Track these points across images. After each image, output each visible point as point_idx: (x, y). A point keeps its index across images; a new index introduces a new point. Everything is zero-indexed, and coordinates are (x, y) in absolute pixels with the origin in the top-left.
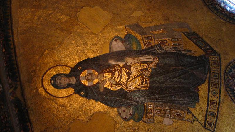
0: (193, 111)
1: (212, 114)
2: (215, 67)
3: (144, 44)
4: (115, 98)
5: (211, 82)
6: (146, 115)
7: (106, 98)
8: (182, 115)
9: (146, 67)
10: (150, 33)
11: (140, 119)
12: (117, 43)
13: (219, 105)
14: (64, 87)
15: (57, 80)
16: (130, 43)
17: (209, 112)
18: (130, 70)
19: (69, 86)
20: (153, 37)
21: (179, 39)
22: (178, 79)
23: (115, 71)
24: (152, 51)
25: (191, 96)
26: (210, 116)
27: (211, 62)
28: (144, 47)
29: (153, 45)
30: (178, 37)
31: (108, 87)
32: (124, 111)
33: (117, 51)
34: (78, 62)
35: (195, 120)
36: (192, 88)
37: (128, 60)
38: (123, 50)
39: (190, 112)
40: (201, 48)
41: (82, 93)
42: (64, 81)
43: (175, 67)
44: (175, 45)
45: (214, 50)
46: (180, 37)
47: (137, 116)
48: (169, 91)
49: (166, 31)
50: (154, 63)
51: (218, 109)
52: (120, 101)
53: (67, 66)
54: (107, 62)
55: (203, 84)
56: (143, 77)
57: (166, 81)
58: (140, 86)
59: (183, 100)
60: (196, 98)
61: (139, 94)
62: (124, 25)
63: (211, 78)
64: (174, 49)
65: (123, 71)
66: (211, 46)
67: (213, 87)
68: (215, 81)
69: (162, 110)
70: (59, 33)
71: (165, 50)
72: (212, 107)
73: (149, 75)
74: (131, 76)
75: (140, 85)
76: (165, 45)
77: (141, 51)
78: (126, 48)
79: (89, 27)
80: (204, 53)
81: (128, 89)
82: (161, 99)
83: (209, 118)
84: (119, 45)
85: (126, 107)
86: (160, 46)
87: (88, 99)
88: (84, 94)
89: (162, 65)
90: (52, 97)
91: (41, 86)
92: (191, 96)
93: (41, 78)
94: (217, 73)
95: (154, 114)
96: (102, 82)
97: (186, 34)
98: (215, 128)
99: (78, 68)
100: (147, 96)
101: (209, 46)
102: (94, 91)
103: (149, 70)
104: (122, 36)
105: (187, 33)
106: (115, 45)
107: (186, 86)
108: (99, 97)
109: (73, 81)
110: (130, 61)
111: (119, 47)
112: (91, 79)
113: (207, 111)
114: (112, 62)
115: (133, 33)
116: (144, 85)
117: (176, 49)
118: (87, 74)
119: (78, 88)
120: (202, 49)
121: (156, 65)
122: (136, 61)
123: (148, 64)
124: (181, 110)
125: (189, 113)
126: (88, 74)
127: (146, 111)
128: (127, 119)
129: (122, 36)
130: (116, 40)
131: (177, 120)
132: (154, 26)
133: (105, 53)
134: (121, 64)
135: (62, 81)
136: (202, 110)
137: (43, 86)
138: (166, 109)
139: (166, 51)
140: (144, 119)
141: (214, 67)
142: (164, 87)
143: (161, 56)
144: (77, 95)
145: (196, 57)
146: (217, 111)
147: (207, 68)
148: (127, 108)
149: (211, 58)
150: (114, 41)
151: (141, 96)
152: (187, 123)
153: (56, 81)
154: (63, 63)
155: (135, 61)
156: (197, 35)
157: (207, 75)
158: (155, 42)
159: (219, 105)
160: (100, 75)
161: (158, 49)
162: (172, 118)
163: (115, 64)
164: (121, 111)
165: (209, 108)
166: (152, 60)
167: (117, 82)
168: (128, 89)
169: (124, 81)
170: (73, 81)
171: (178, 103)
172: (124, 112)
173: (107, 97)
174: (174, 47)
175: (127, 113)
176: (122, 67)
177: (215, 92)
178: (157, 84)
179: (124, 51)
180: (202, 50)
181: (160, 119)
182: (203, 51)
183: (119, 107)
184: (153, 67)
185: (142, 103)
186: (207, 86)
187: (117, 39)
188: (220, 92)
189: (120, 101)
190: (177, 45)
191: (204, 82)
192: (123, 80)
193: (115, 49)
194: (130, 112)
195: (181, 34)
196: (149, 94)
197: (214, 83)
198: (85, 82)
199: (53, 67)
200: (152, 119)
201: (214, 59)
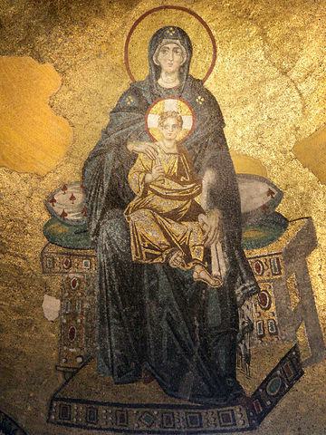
7: (110, 156)
11: (51, 238)
14: (154, 59)
18: (185, 219)
23: (183, 183)
24: (241, 274)
30: (282, 335)
32: (72, 198)
33: (241, 193)
45: (265, 416)
48: (133, 311)
50: (208, 278)
51: (107, 429)
52: (101, 190)
55: (165, 391)
56: (166, 249)
59: (114, 345)
69: (80, 294)
73: (171, 265)
76: (256, 306)
93: (188, 7)
96: (153, 150)
98: (59, 424)
100: (115, 257)
101: (273, 406)
102: (132, 127)
106: (257, 190)
107: (152, 353)
109: (168, 81)
110: (211, 221)
111: (252, 198)
112: (165, 123)
115: (292, 231)
122: (210, 236)
124: (86, 340)
125: (80, 360)
129: (282, 209)
130: (270, 193)
134: (202, 200)
140: (53, 249)
144: (125, 87)
145: (233, 375)
148: (81, 205)
156: (298, 379)
160: (173, 147)
161: (245, 288)
166: (215, 272)
168: (134, 211)
169: (154, 203)
170: (168, 81)
171: (102, 334)
173: (111, 159)
174: (253, 324)
178: (149, 282)
180: (258, 390)
183: (82, 186)
184: (195, 276)
192: (157, 202)
201: (239, 416)
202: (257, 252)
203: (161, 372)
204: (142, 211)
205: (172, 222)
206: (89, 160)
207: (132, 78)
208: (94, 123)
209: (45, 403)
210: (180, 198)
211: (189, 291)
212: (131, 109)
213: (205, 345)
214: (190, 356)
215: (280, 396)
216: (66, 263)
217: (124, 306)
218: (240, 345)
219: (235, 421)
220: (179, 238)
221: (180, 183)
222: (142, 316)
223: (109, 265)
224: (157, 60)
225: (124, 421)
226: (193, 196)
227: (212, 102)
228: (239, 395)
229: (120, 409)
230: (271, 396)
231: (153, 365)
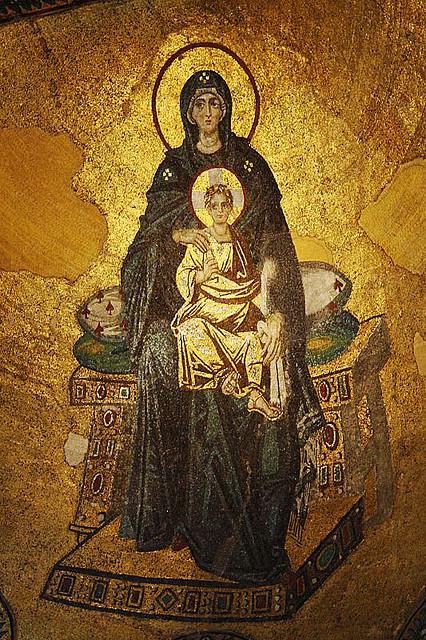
0: (111, 530)
1: (99, 592)
7: (153, 251)
9: (250, 380)
11: (83, 358)
13: (129, 614)
15: (211, 93)
16: (328, 331)
17: (107, 583)
18: (244, 327)
19: (192, 130)
22: (213, 484)
23: (239, 281)
24: (304, 401)
27: (267, 590)
28: (315, 375)
29: (323, 405)
31: (187, 255)
32: (110, 307)
34: (269, 159)
37: (274, 323)
39: (106, 522)
40: (313, 557)
41: (168, 174)
42: (207, 116)
48: (175, 454)
49: (366, 448)
52: (143, 295)
53: (255, 124)
54: (269, 255)
56: (220, 370)
57: (206, 445)
58: (190, 360)
63: (216, 590)
64: (308, 470)
65: (237, 308)
67: (187, 596)
68: (205, 601)
70: (361, 100)
73: (224, 391)
74: (223, 331)
75: (193, 360)
76: (321, 444)
77: (304, 367)
78: (313, 315)
79: (380, 198)
80: (295, 568)
85: (124, 315)
87: (147, 193)
90: (155, 75)
91: (191, 39)
93: (218, 40)
96: (203, 240)
97: (357, 510)
98: (55, 600)
100: (159, 383)
101: (319, 585)
104: (350, 306)
106: (323, 282)
109: (208, 145)
110: (272, 328)
112: (213, 202)
113: (110, 575)
114: (268, 270)
115: (362, 338)
116: (194, 373)
122: (270, 351)
124: (113, 492)
126: (230, 194)
127: (109, 381)
129: (350, 306)
130: (338, 285)
131: (79, 477)
134: (261, 301)
137: (193, 46)
138: (116, 442)
139: (302, 447)
140: (85, 374)
143: (286, 428)
144: (161, 157)
145: (282, 542)
150: (337, 277)
152: (71, 510)
153: (209, 89)
154: (265, 112)
157: (223, 576)
158: (327, 409)
159: (129, 614)
161: (308, 419)
166: (274, 399)
167: (203, 287)
168: (182, 321)
169: (205, 309)
170: (208, 145)
171: (134, 484)
176: (251, 304)
178: (197, 415)
180: (307, 562)
181: (84, 424)
185: (135, 366)
186: (189, 578)
187: (342, 289)
188: (169, 618)
189: (143, 295)
191: (203, 568)
193: (310, 280)
194: (106, 327)
197: (199, 598)
198: (203, 181)
199: (252, 80)
201: (277, 598)
202: (325, 369)
210: (238, 301)
211: (242, 426)
213: (256, 499)
215: (328, 573)
216: (100, 392)
219: (270, 605)
220: (235, 355)
221: (236, 280)
224: (191, 117)
226: (244, 300)
227: (262, 166)
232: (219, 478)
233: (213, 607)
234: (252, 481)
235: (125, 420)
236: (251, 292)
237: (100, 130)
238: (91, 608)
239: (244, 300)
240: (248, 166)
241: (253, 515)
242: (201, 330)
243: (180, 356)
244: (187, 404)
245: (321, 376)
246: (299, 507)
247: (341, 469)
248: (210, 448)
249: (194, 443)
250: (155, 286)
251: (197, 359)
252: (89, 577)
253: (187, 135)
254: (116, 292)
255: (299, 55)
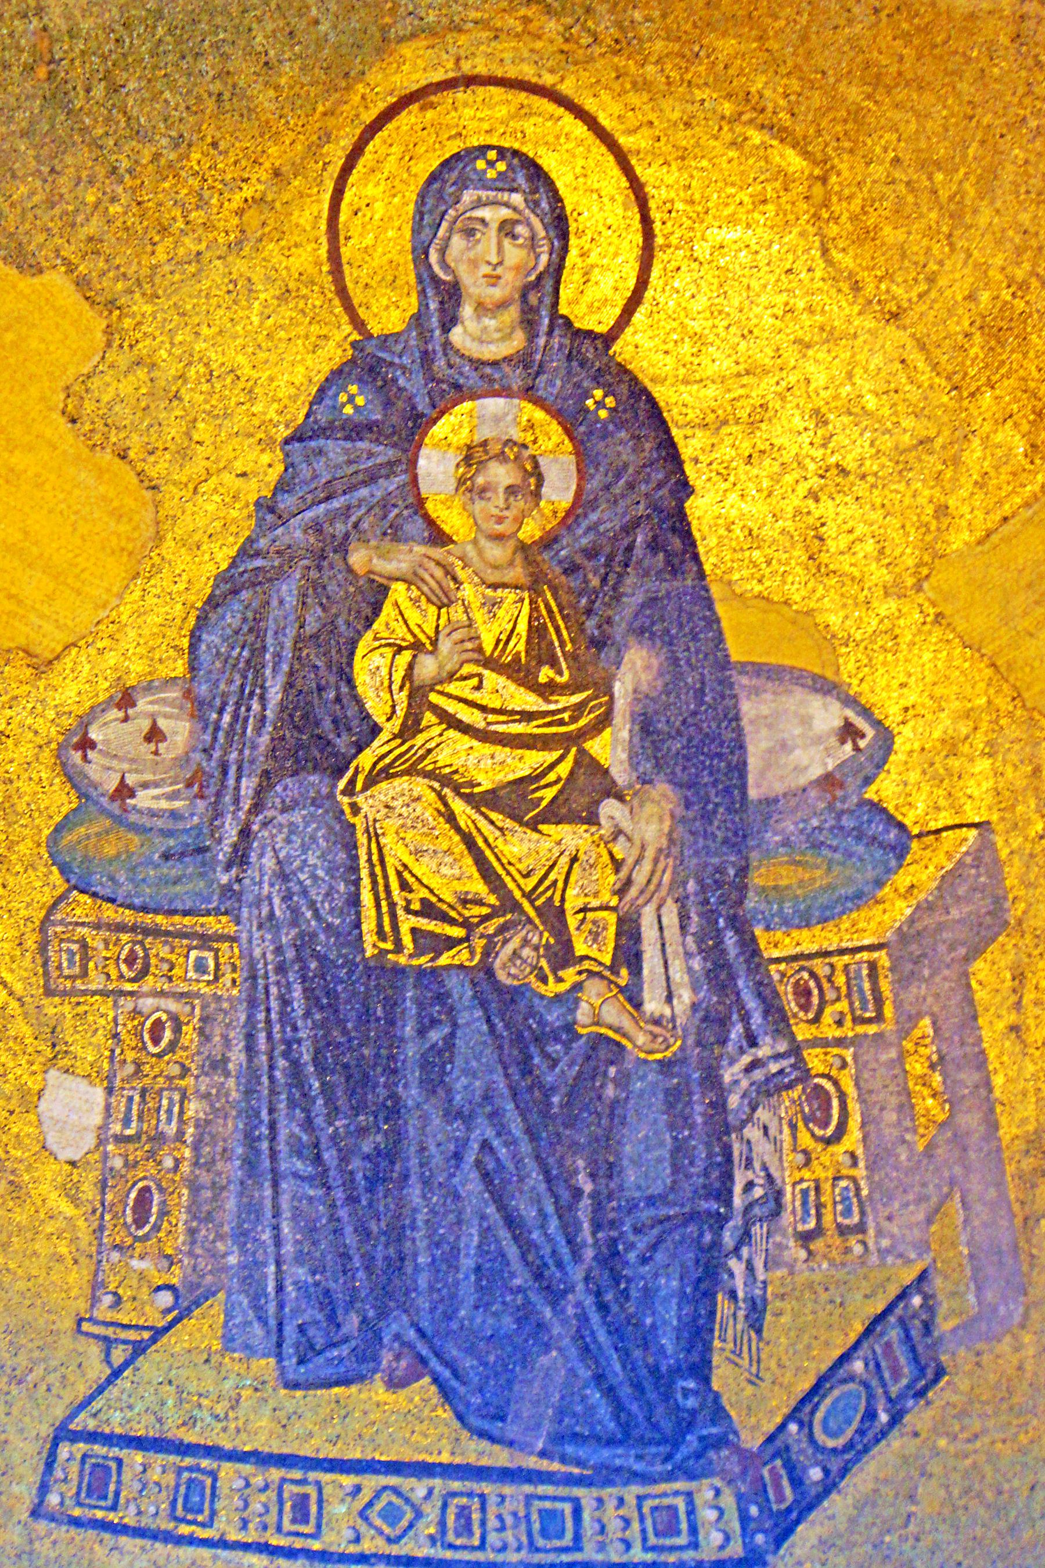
2: (636, 1525)
3: (810, 957)
4: (285, 667)
5: (487, 1488)
6: (121, 928)
7: (288, 591)
8: (137, 1239)
9: (581, 948)
10: (920, 1016)
12: (818, 740)
14: (434, 257)
15: (507, 205)
17: (214, 1475)
18: (553, 814)
20: (879, 1036)
21: (864, 1243)
23: (547, 690)
25: (332, 1318)
26: (170, 1479)
27: (676, 1493)
28: (776, 954)
29: (802, 1032)
30: (879, 1233)
31: (388, 610)
32: (154, 735)
33: (748, 728)
35: (119, 1355)
36: (412, 1333)
37: (650, 808)
38: (751, 779)
39: (181, 1313)
43: (594, 1195)
44: (805, 1203)
45: (798, 1522)
46: (883, 1253)
47: (110, 850)
48: (362, 1132)
49: (930, 1146)
50: (627, 1024)
51: (246, 1547)
52: (256, 706)
55: (460, 1417)
56: (485, 918)
57: (452, 1114)
60: (320, 1360)
61: (314, 877)
62: (995, 818)
63: (528, 1489)
64: (758, 1192)
65: (534, 759)
66: (834, 1496)
67: (445, 1506)
68: (500, 1517)
69: (176, 1070)
71: (749, 1119)
72: (263, 1498)
73: (501, 976)
74: (494, 816)
76: (793, 1127)
78: (771, 802)
79: (995, 538)
80: (752, 1441)
81: (365, 788)
82: (282, 1063)
83: (155, 1475)
84: (798, 752)
85: (197, 756)
86: (789, 1086)
87: (287, 441)
88: (348, 410)
89: (610, 1091)
91: (466, 67)
92: (332, 1318)
93: (548, 80)
94: (577, 1537)
95: (131, 994)
96: (439, 573)
97: (917, 1300)
98: (76, 1522)
99: (599, 385)
100: (304, 943)
101: (829, 1487)
102: (364, 492)
103: (560, 980)
105: (929, 1306)
106: (806, 721)
107: (423, 1281)
108: (298, 534)
111: (784, 746)
112: (480, 480)
117: (757, 1211)
118: (533, 458)
119: (403, 368)
120: (793, 1427)
121: (608, 1039)
122: (640, 877)
123: (614, 969)
124: (192, 1232)
125: (166, 1299)
126: (536, 466)
127: (156, 932)
128: (77, 756)
130: (848, 732)
131: (89, 1192)
132: (983, 1052)
133: (725, 624)
135: (494, 241)
136: (219, 1409)
138: (184, 1097)
139: (741, 1129)
140: (82, 906)
141: (630, 1510)
142: (394, 1096)
145: (702, 1370)
146: (233, 1536)
147: (618, 1462)
149: (718, 1492)
150: (850, 714)
151: (296, 888)
152: (78, 1278)
153: (505, 196)
155: (638, 862)
156: (921, 1394)
157: (543, 1454)
158: (824, 1043)
160: (511, 564)
162: (105, 1156)
163: (612, 697)
164: (151, 708)
165: (247, 1468)
166: (653, 1005)
167: (434, 698)
168: (371, 781)
169: (442, 757)
171: (251, 1209)
172: (148, 739)
173: (291, 601)
174: (779, 1194)
175: (133, 761)
176: (582, 752)
177: (404, 1523)
178: (422, 1032)
179: (743, 788)
180: (782, 1427)
182: (769, 1427)
183: (187, 694)
184: (583, 1015)
186: (445, 1458)
189: (256, 706)
190: (804, 1221)
191: (482, 1434)
193: (765, 710)
194: (145, 786)
195: (908, 1262)
196: (321, 958)
197: (483, 1509)
200: (84, 974)
201: (711, 1515)
202: (808, 940)
203: (453, 1352)
204: (402, 784)
205: (509, 823)
206: (212, 603)
207: (358, 324)
208: (227, 478)
209: (31, 1448)
212: (355, 430)
214: (555, 1296)
216: (130, 961)
217: (333, 1112)
218: (733, 1263)
219: (693, 1530)
222: (389, 1154)
223: (281, 969)
225: (305, 1520)
226: (568, 741)
228: (720, 1442)
229: (297, 1474)
230: (823, 1450)
231: (425, 1324)
232: (499, 1200)
233: (530, 1534)
234: (598, 1207)
235: (204, 1035)
236: (582, 722)
237: (167, 268)
238: (180, 1541)
239: (568, 741)
240: (600, 404)
241: (609, 1297)
242: (427, 809)
243: (364, 873)
244: (392, 1004)
245: (795, 958)
246: (739, 1283)
247: (858, 1194)
248: (467, 1119)
249: (418, 1106)
250: (289, 685)
251: (415, 886)
252: (160, 1459)
253: (423, 305)
254: (174, 694)
255: (790, 153)
